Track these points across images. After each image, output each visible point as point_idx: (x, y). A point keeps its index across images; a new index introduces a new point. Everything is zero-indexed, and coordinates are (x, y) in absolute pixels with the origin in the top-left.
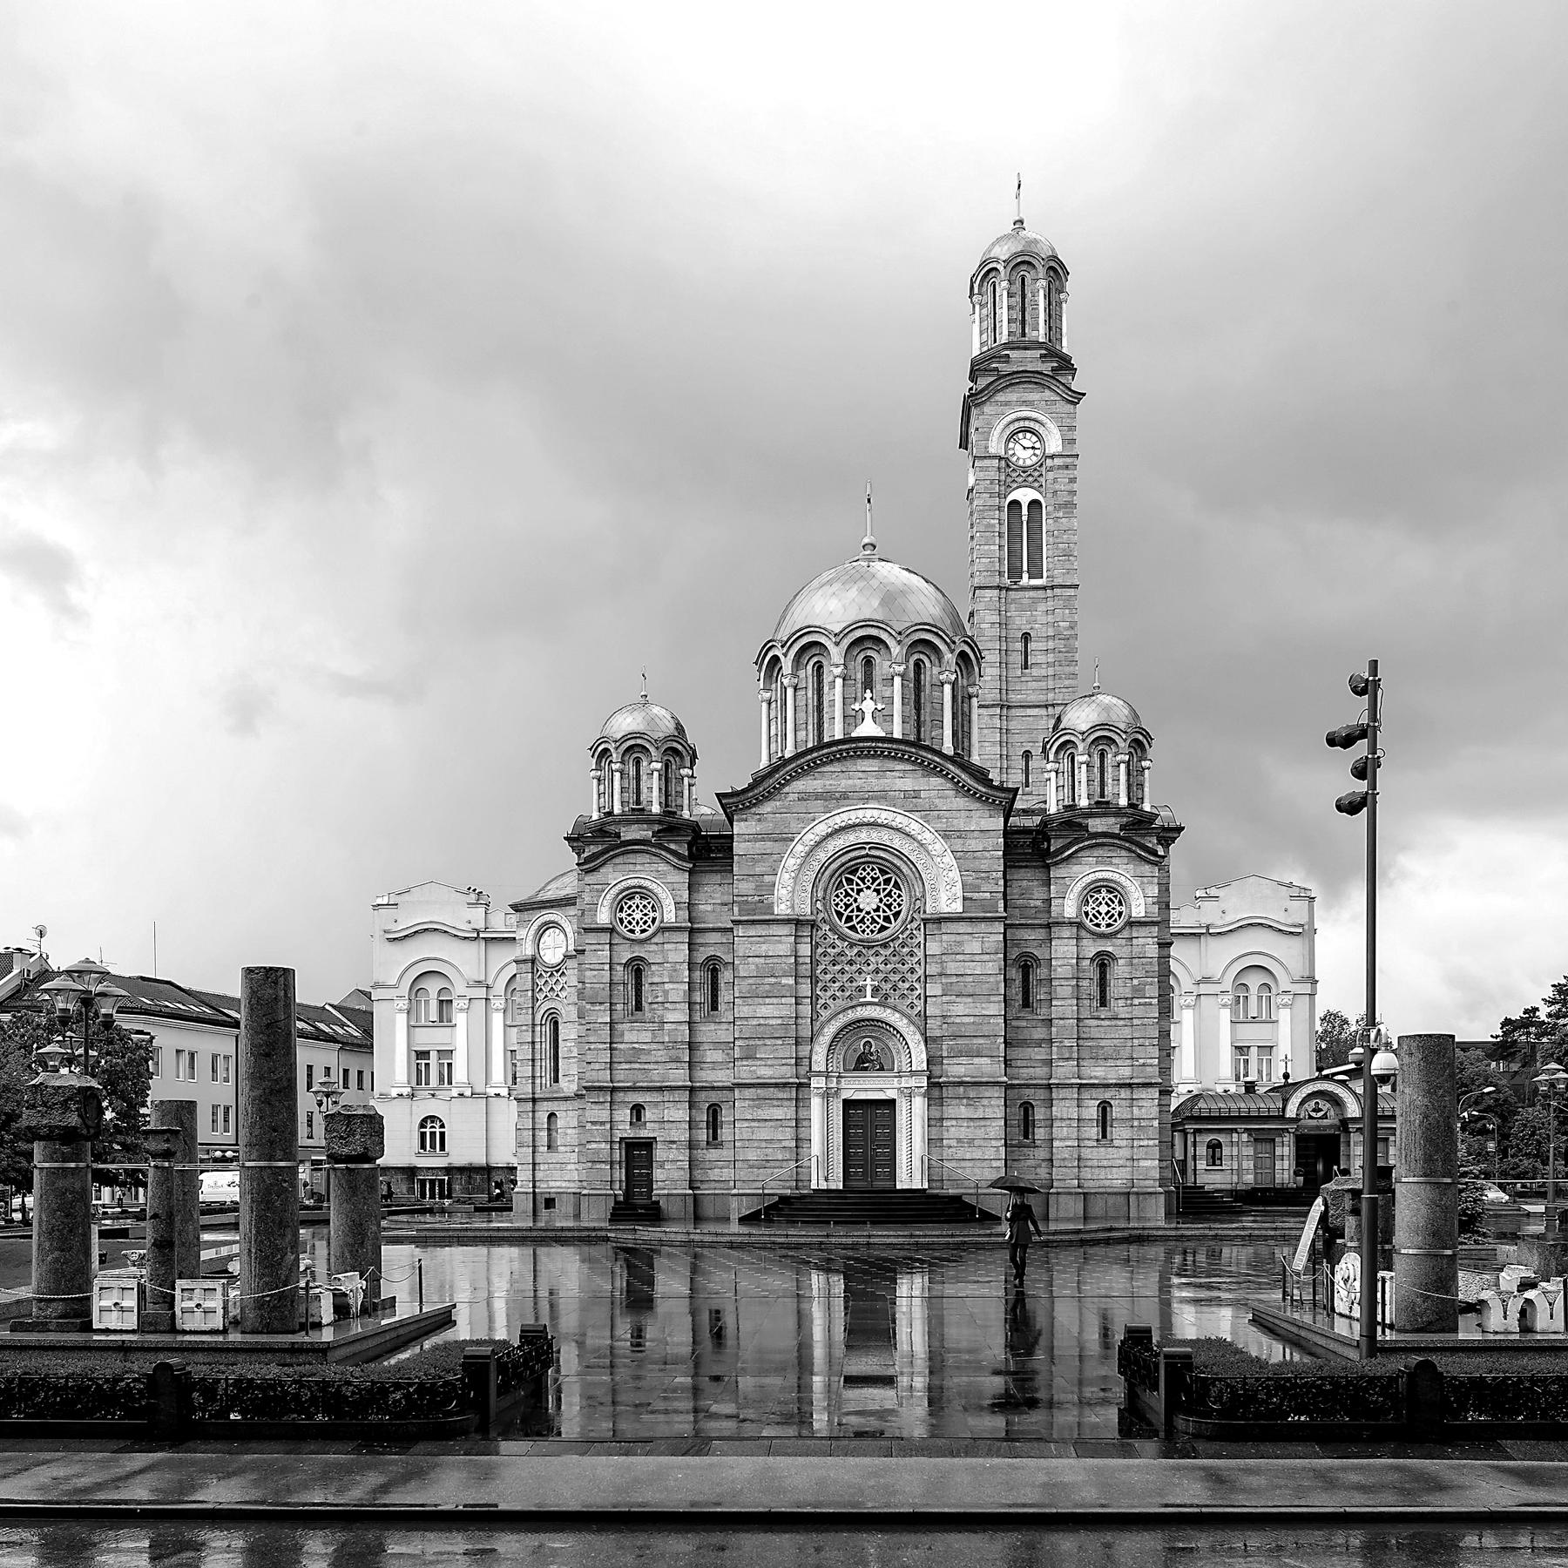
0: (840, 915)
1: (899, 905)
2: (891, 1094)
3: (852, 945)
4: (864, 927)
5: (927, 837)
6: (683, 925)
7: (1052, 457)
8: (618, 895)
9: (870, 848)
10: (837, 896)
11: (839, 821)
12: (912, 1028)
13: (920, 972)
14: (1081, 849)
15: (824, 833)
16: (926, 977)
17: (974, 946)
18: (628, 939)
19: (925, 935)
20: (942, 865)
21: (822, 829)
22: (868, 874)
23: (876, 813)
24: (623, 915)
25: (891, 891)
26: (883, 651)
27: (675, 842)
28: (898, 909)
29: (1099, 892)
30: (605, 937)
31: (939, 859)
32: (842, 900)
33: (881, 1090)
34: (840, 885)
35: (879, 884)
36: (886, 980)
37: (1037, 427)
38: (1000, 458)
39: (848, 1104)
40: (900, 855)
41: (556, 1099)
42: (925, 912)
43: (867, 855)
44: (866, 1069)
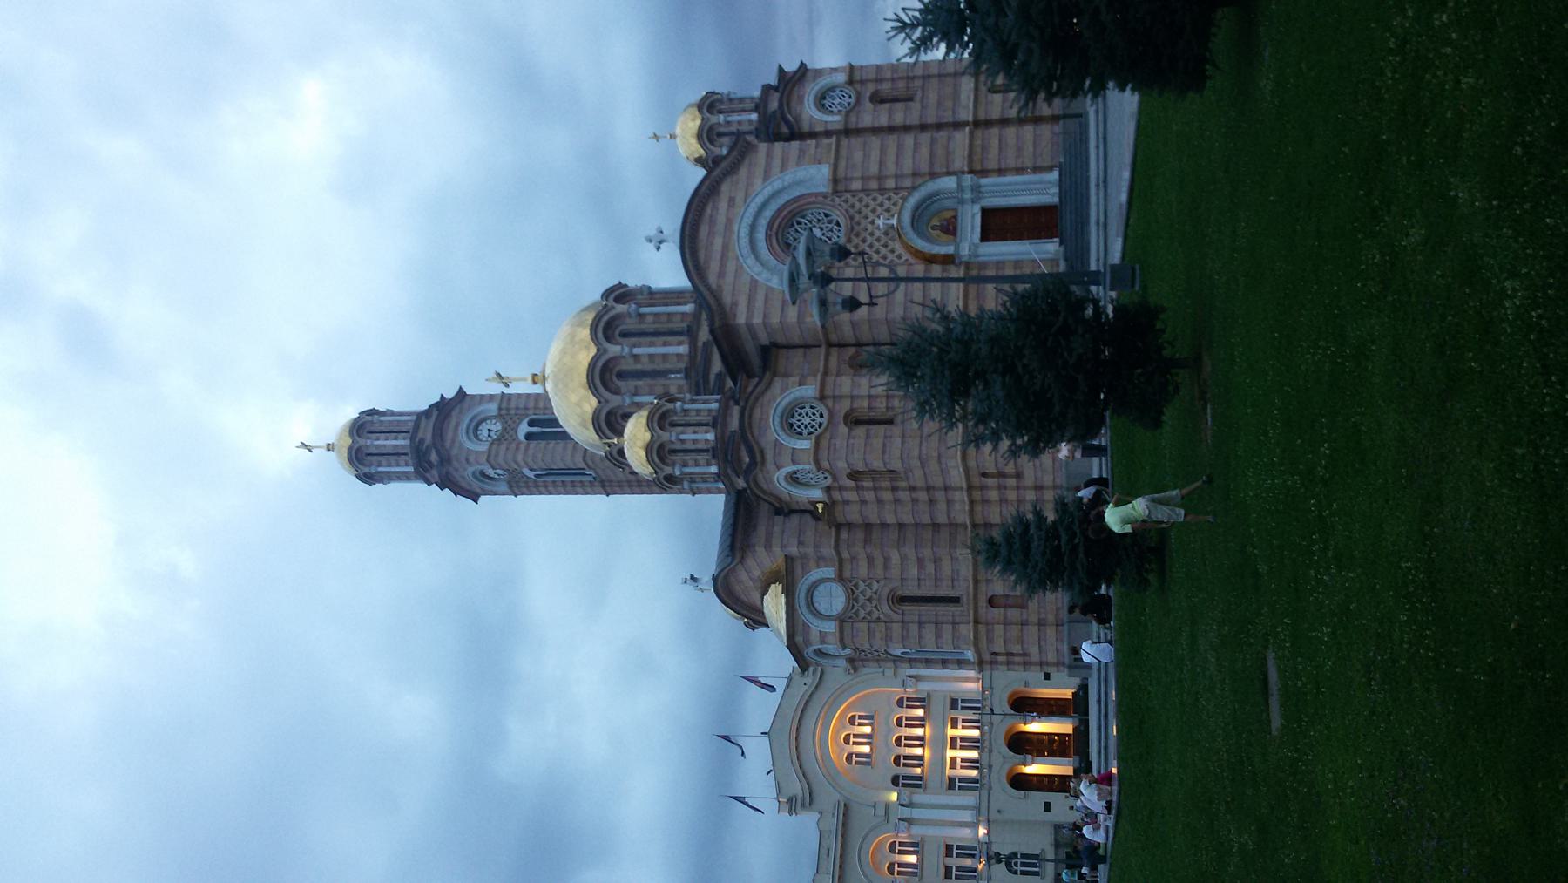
2: (977, 209)
5: (768, 191)
6: (819, 378)
7: (500, 409)
8: (786, 433)
9: (771, 230)
11: (746, 250)
13: (876, 194)
14: (790, 114)
15: (754, 260)
17: (858, 156)
18: (828, 425)
19: (846, 191)
21: (751, 261)
23: (744, 224)
24: (805, 432)
26: (616, 323)
27: (746, 387)
29: (824, 105)
30: (824, 443)
33: (973, 216)
37: (476, 421)
38: (492, 443)
39: (985, 237)
40: (779, 211)
41: (976, 596)
42: (827, 193)
44: (955, 229)
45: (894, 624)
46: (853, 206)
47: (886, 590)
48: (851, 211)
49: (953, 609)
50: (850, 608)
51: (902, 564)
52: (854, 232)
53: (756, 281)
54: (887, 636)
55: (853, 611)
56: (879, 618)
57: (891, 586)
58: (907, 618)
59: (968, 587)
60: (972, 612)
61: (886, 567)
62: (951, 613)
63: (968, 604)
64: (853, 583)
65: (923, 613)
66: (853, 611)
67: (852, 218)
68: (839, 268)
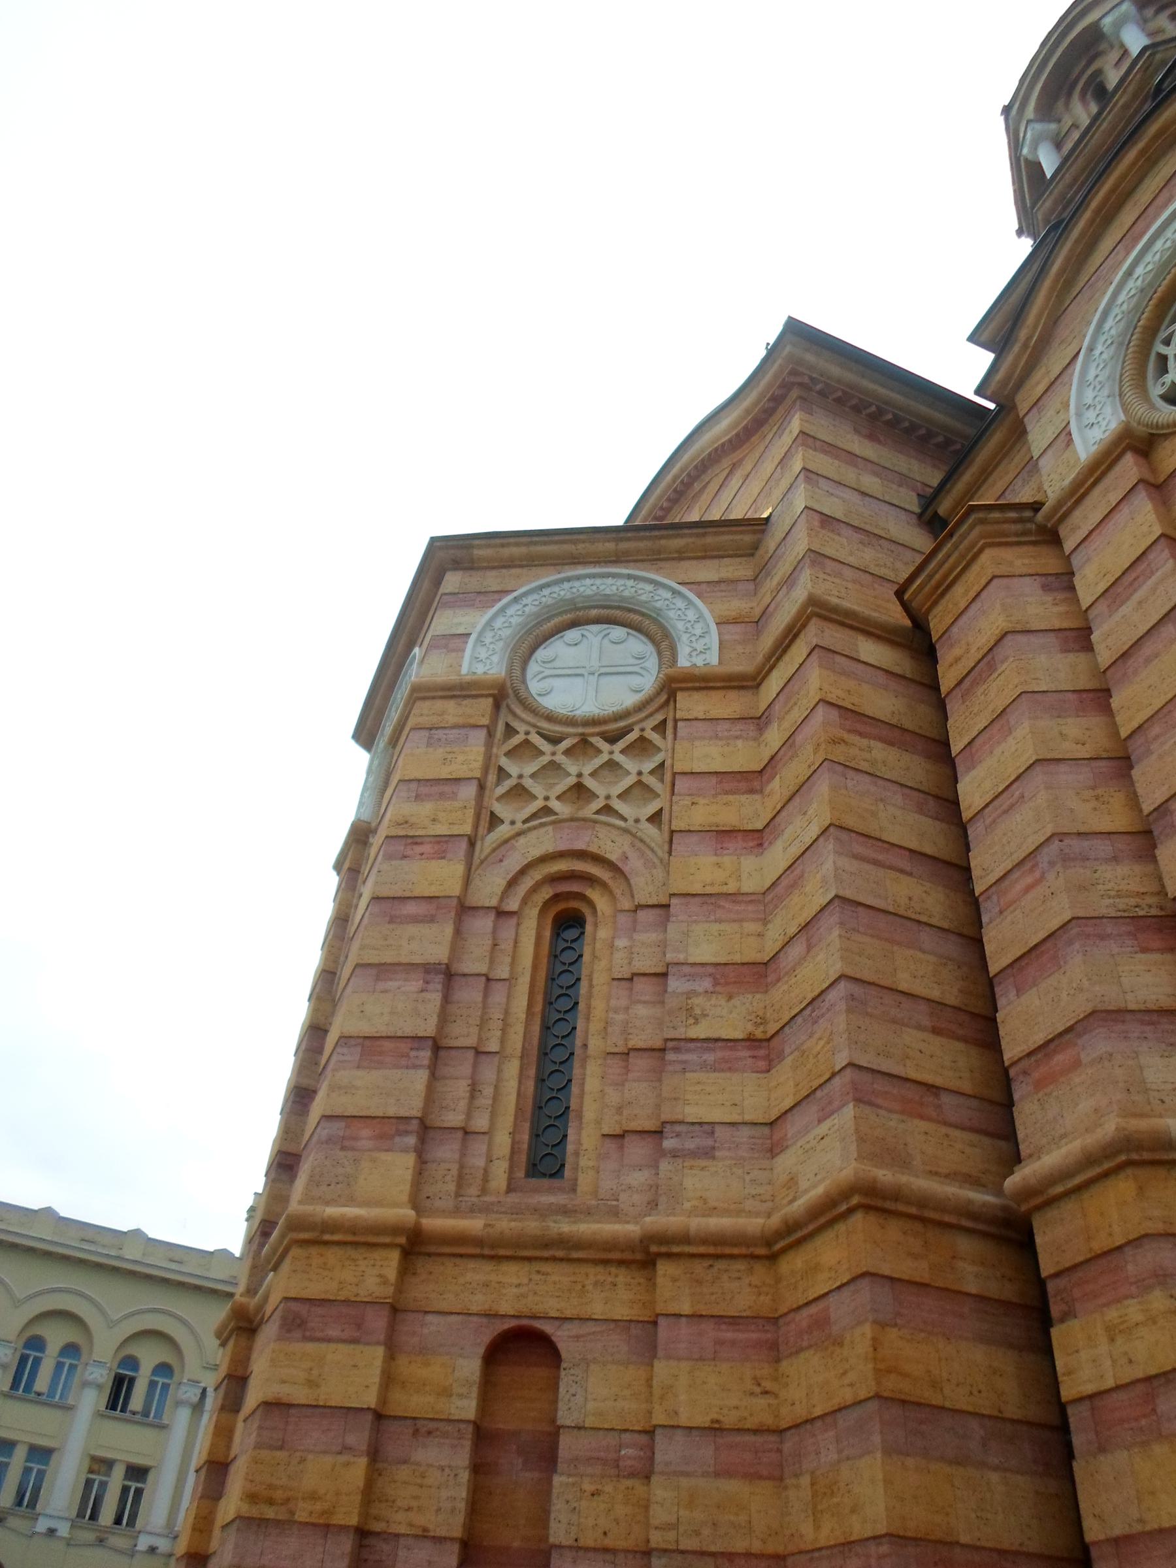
45: (459, 869)
47: (611, 845)
49: (503, 1141)
50: (544, 725)
51: (735, 897)
54: (415, 841)
55: (535, 739)
56: (495, 821)
57: (634, 864)
58: (483, 924)
59: (615, 1213)
60: (474, 1225)
61: (724, 835)
62: (481, 1122)
63: (516, 1212)
64: (655, 737)
65: (498, 996)
66: (535, 739)
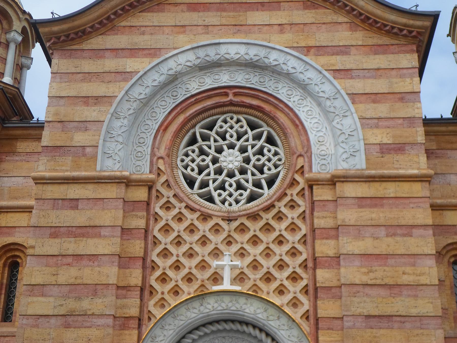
0: (191, 183)
1: (276, 166)
3: (205, 217)
4: (224, 194)
9: (235, 94)
10: (187, 155)
12: (295, 332)
16: (315, 259)
19: (313, 202)
20: (332, 110)
22: (232, 127)
25: (262, 148)
28: (274, 171)
31: (328, 103)
32: (193, 161)
34: (193, 141)
35: (247, 140)
36: (255, 265)
43: (231, 104)
46: (279, 217)
48: (268, 217)
52: (224, 224)
53: (126, 80)
67: (254, 217)
68: (148, 204)
